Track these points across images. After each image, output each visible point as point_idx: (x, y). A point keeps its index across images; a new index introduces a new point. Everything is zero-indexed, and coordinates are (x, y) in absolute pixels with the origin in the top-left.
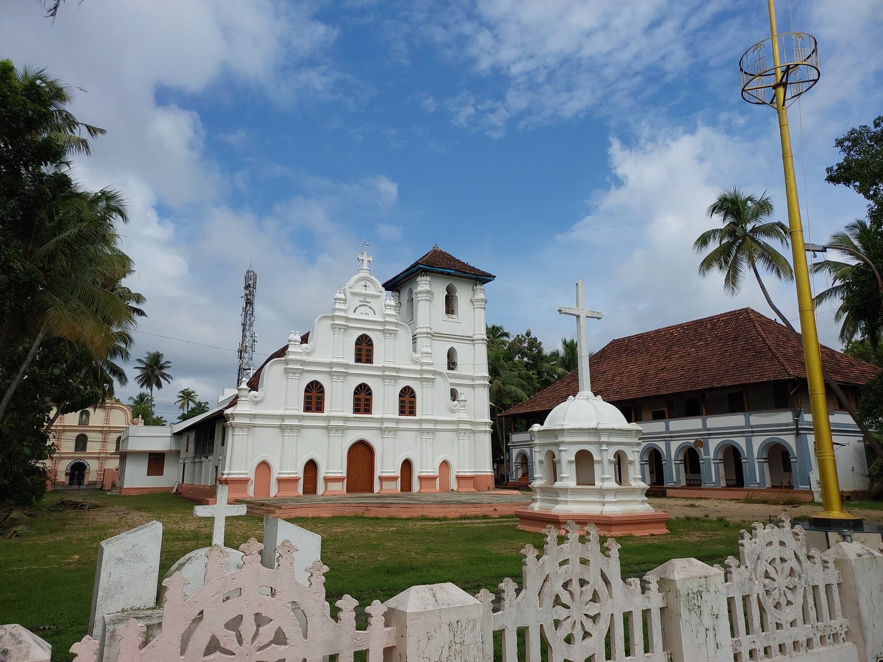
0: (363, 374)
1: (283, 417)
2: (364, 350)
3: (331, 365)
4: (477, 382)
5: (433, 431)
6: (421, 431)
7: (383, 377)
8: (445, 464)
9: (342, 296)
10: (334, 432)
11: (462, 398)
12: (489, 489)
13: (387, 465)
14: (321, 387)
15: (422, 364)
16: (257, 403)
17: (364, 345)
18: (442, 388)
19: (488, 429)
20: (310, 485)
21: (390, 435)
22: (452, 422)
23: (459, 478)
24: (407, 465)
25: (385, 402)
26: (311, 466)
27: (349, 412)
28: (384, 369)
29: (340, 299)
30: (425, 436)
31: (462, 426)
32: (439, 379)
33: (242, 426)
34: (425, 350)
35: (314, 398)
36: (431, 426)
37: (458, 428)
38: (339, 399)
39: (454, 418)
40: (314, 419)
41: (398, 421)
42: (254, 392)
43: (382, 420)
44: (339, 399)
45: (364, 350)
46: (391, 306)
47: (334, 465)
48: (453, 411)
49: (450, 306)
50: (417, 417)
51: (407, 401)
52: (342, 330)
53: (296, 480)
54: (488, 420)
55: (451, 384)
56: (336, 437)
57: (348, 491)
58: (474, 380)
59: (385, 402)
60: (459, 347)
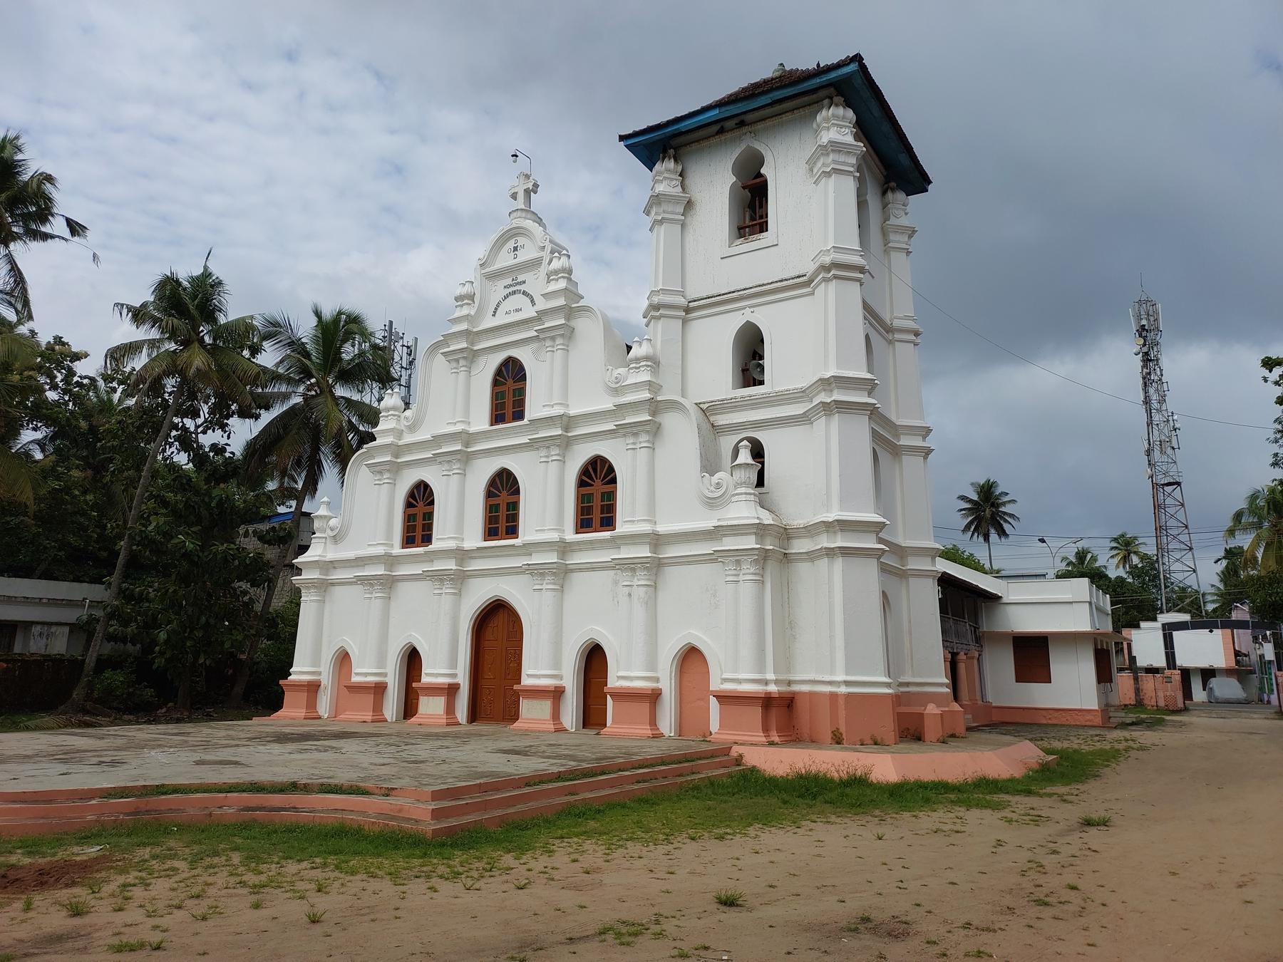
8: (691, 657)
24: (594, 658)
60: (763, 317)
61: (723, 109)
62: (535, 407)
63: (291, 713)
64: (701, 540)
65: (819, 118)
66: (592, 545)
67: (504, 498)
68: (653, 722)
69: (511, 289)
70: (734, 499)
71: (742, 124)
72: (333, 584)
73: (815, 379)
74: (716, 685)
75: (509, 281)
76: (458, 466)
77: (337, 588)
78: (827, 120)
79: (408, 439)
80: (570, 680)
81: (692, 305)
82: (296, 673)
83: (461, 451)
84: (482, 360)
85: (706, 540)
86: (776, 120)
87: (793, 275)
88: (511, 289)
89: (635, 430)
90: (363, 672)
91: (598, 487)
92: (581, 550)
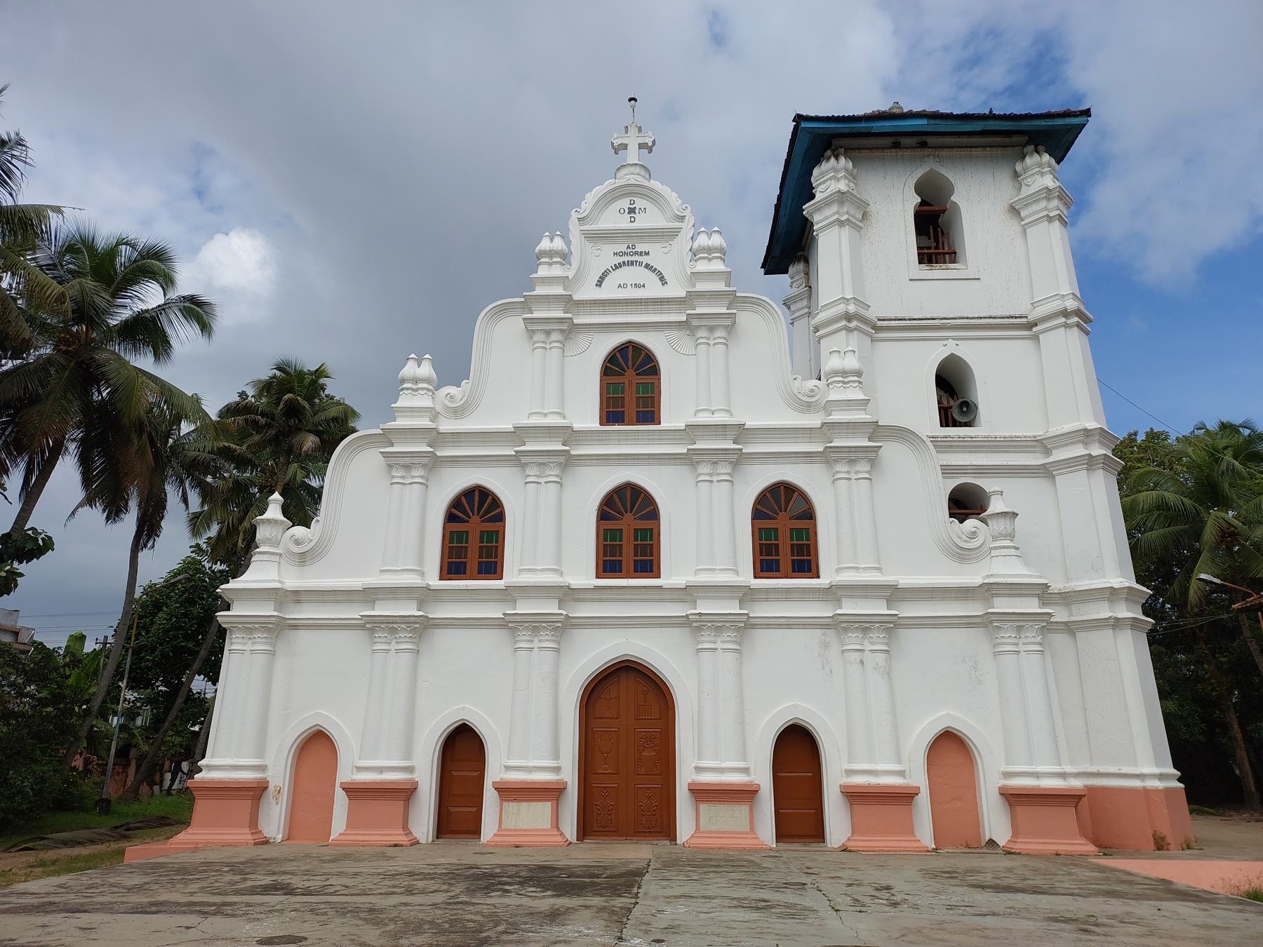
1: (370, 595)
2: (630, 385)
3: (520, 434)
4: (1059, 455)
5: (892, 626)
6: (839, 625)
7: (690, 459)
8: (949, 746)
9: (558, 244)
11: (995, 506)
12: (1160, 844)
13: (719, 743)
14: (496, 503)
15: (829, 406)
16: (303, 559)
17: (630, 373)
18: (917, 483)
19: (1127, 612)
20: (458, 815)
21: (724, 642)
22: (964, 593)
23: (1015, 799)
24: (797, 747)
25: (705, 534)
26: (462, 747)
27: (582, 573)
28: (693, 430)
29: (551, 253)
30: (853, 640)
31: (1003, 605)
32: (891, 451)
33: (251, 626)
34: (832, 363)
37: (989, 613)
38: (550, 536)
39: (972, 576)
40: (472, 599)
41: (746, 595)
42: (299, 531)
43: (688, 593)
44: (550, 536)
45: (630, 385)
46: (709, 250)
47: (534, 742)
48: (963, 555)
49: (935, 235)
51: (784, 535)
52: (555, 336)
53: (406, 793)
54: (1120, 575)
55: (947, 471)
56: (537, 657)
57: (585, 830)
58: (1048, 452)
59: (705, 534)
60: (972, 352)
61: (932, 122)
62: (676, 408)
63: (204, 836)
64: (950, 599)
65: (1029, 161)
66: (787, 594)
67: (475, 526)
68: (253, 823)
69: (626, 259)
70: (994, 553)
71: (923, 145)
72: (295, 627)
73: (1081, 427)
74: (346, 774)
75: (623, 248)
76: (557, 472)
77: (303, 635)
78: (1040, 165)
79: (446, 426)
80: (759, 770)
81: (880, 323)
82: (211, 768)
83: (557, 454)
84: (582, 339)
85: (956, 599)
86: (966, 152)
87: (1003, 314)
88: (626, 259)
89: (853, 456)
90: (360, 761)
91: (475, 526)
92: (767, 600)
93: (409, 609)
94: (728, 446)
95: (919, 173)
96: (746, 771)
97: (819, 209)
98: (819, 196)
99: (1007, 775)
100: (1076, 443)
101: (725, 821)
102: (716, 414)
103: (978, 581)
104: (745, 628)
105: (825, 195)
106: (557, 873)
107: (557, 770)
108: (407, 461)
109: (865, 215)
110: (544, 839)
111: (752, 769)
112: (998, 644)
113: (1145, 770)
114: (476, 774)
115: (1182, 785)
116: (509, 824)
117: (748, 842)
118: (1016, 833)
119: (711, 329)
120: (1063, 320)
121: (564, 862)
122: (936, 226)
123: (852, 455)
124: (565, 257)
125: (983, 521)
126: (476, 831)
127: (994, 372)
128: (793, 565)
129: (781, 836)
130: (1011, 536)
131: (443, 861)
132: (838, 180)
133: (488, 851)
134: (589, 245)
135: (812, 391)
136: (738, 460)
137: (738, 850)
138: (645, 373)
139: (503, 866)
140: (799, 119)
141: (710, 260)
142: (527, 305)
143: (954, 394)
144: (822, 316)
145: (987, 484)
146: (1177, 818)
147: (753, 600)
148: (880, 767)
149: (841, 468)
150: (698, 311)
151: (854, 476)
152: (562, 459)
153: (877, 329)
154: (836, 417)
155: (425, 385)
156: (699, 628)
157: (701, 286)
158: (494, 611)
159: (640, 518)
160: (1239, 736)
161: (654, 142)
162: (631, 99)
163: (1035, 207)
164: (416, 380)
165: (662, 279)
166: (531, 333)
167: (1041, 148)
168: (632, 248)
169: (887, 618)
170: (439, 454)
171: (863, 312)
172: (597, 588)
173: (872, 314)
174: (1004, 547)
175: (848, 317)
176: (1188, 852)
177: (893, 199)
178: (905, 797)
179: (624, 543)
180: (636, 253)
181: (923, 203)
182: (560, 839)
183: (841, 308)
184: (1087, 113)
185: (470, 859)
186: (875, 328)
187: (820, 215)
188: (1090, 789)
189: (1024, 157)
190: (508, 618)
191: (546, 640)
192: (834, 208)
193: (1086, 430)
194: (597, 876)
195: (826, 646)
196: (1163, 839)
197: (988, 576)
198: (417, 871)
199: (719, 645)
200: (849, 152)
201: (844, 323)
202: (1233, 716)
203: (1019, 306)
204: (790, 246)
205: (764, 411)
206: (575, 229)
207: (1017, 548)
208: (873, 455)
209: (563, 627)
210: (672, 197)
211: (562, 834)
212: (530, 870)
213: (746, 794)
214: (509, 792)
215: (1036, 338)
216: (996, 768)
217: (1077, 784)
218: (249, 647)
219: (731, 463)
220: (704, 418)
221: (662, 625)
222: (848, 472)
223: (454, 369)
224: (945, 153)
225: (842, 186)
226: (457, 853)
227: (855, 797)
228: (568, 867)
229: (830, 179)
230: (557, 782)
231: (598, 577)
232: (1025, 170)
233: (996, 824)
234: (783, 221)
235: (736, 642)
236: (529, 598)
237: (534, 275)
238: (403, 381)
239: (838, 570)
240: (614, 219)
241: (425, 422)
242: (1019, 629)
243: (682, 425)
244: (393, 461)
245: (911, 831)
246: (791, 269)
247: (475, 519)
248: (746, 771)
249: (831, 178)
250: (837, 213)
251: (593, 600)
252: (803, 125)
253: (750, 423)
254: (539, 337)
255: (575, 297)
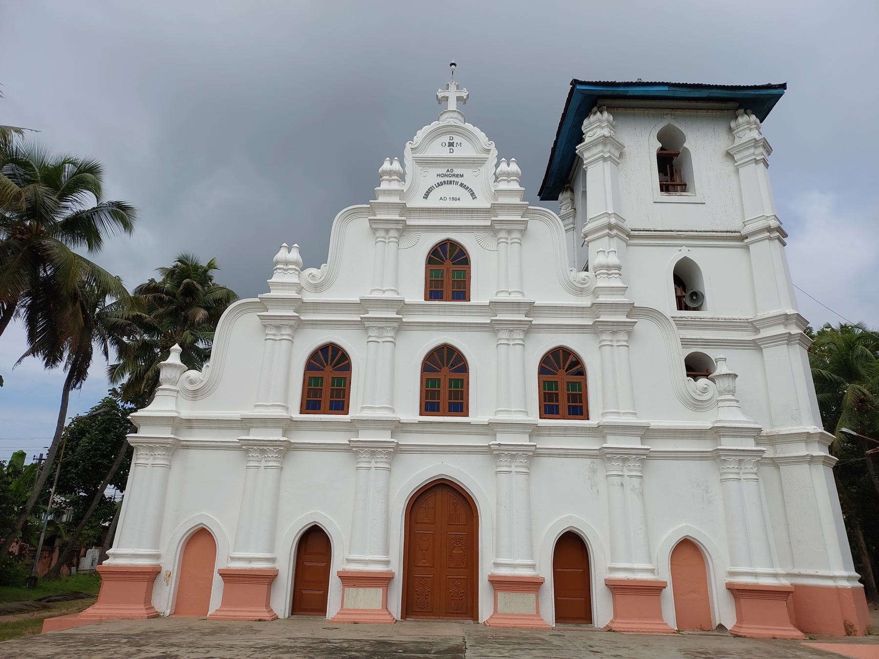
0: (445, 326)
1: (246, 423)
2: (448, 270)
3: (364, 304)
4: (765, 333)
7: (493, 328)
8: (687, 550)
9: (396, 166)
10: (364, 457)
11: (721, 369)
12: (849, 631)
15: (596, 292)
16: (195, 395)
17: (448, 263)
18: (661, 348)
19: (820, 451)
20: (309, 596)
23: (738, 592)
24: (571, 548)
25: (504, 385)
26: (314, 543)
27: (409, 409)
28: (495, 305)
29: (390, 173)
30: (615, 468)
31: (727, 443)
32: (643, 326)
33: (153, 445)
34: (601, 259)
35: (327, 381)
36: (634, 443)
37: (716, 448)
38: (387, 382)
39: (704, 421)
41: (534, 431)
42: (193, 373)
43: (491, 428)
44: (387, 382)
45: (448, 270)
46: (508, 174)
47: (370, 542)
48: (697, 405)
49: (672, 171)
50: (593, 422)
51: (563, 386)
52: (393, 233)
53: (269, 578)
54: (814, 425)
55: (685, 342)
57: (409, 609)
58: (757, 330)
59: (504, 385)
60: (700, 256)
61: (671, 89)
62: (482, 291)
63: (107, 613)
64: (688, 438)
65: (741, 120)
69: (446, 179)
70: (720, 404)
72: (187, 447)
75: (444, 171)
76: (392, 334)
77: (194, 454)
78: (749, 123)
79: (309, 297)
80: (543, 568)
82: (116, 556)
84: (412, 237)
85: (693, 438)
86: (694, 113)
87: (722, 230)
88: (446, 179)
89: (615, 328)
92: (549, 435)
93: (276, 435)
94: (522, 319)
95: (660, 125)
96: (533, 566)
97: (588, 149)
98: (587, 140)
99: (733, 574)
100: (779, 324)
101: (517, 605)
102: (512, 295)
103: (708, 425)
104: (533, 456)
105: (593, 138)
106: (394, 648)
107: (387, 563)
108: (278, 322)
109: (621, 155)
110: (377, 617)
111: (537, 565)
112: (725, 473)
113: (837, 573)
114: (324, 564)
115: (862, 585)
116: (349, 604)
117: (535, 623)
118: (740, 618)
119: (509, 232)
120: (768, 234)
121: (396, 638)
122: (671, 167)
123: (615, 328)
124: (402, 177)
125: (712, 380)
126: (322, 609)
127: (715, 270)
128: (569, 410)
129: (559, 618)
130: (733, 392)
131: (299, 635)
132: (602, 128)
133: (334, 626)
134: (419, 169)
135: (584, 280)
136: (529, 329)
137: (527, 629)
138: (459, 263)
139: (348, 641)
140: (575, 82)
141: (509, 181)
142: (372, 210)
143: (687, 288)
144: (589, 226)
145: (712, 353)
146: (857, 611)
147: (538, 435)
148: (636, 566)
149: (606, 337)
150: (500, 218)
151: (615, 344)
152: (396, 325)
153: (631, 236)
154: (602, 299)
155: (294, 267)
156: (498, 456)
157: (502, 200)
158: (342, 439)
159: (454, 371)
160: (864, 546)
161: (468, 96)
162: (452, 64)
163: (746, 153)
164: (287, 263)
165: (473, 194)
166: (375, 230)
167: (748, 111)
168: (450, 172)
169: (639, 451)
170: (302, 318)
171: (621, 224)
172: (420, 423)
173: (628, 225)
174: (728, 400)
175: (610, 227)
176: (871, 637)
177: (642, 144)
178: (654, 590)
179: (441, 389)
180: (454, 175)
181: (662, 149)
182: (389, 617)
183: (604, 221)
184: (784, 86)
185: (322, 634)
186: (629, 236)
187: (588, 152)
188: (796, 586)
189: (736, 117)
190: (352, 444)
191: (381, 462)
192: (600, 148)
193: (786, 315)
194: (427, 652)
195: (594, 471)
196: (852, 626)
197: (717, 422)
198: (281, 645)
199: (513, 469)
200: (610, 109)
201: (607, 231)
202: (859, 532)
203: (734, 224)
204: (560, 178)
205: (549, 293)
206: (408, 155)
207: (737, 401)
208: (629, 328)
209: (395, 451)
210: (481, 135)
211: (390, 614)
212: (372, 645)
213: (532, 585)
214: (350, 580)
215: (747, 247)
216: (724, 568)
217: (785, 582)
218: (151, 461)
219: (524, 331)
220: (503, 297)
221: (469, 453)
222: (611, 341)
223: (315, 255)
224: (679, 112)
225: (606, 132)
226: (308, 629)
227: (616, 588)
228: (400, 644)
229: (597, 127)
230: (387, 573)
231: (421, 415)
232: (738, 126)
233: (724, 612)
234: (557, 159)
235: (526, 467)
236: (369, 429)
237: (377, 188)
238: (277, 263)
239: (604, 414)
240: (436, 149)
241: (292, 294)
242: (740, 461)
243: (486, 302)
244: (267, 322)
245: (660, 617)
246: (560, 197)
247: (329, 368)
248: (533, 566)
249: (596, 127)
250: (602, 151)
251: (417, 432)
252: (578, 87)
253: (538, 303)
254: (381, 233)
255: (408, 206)
